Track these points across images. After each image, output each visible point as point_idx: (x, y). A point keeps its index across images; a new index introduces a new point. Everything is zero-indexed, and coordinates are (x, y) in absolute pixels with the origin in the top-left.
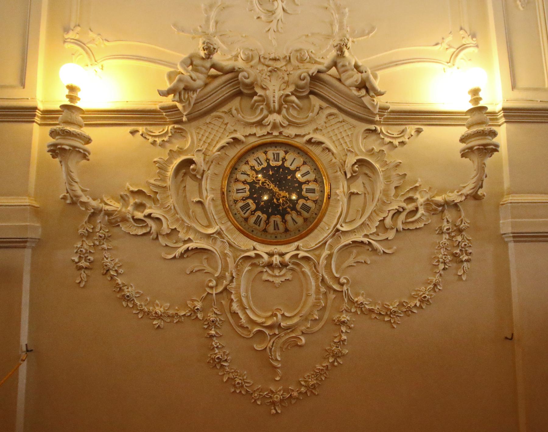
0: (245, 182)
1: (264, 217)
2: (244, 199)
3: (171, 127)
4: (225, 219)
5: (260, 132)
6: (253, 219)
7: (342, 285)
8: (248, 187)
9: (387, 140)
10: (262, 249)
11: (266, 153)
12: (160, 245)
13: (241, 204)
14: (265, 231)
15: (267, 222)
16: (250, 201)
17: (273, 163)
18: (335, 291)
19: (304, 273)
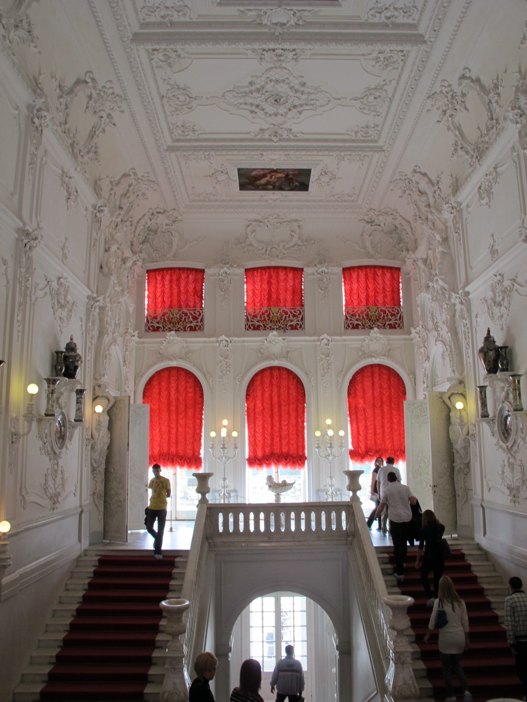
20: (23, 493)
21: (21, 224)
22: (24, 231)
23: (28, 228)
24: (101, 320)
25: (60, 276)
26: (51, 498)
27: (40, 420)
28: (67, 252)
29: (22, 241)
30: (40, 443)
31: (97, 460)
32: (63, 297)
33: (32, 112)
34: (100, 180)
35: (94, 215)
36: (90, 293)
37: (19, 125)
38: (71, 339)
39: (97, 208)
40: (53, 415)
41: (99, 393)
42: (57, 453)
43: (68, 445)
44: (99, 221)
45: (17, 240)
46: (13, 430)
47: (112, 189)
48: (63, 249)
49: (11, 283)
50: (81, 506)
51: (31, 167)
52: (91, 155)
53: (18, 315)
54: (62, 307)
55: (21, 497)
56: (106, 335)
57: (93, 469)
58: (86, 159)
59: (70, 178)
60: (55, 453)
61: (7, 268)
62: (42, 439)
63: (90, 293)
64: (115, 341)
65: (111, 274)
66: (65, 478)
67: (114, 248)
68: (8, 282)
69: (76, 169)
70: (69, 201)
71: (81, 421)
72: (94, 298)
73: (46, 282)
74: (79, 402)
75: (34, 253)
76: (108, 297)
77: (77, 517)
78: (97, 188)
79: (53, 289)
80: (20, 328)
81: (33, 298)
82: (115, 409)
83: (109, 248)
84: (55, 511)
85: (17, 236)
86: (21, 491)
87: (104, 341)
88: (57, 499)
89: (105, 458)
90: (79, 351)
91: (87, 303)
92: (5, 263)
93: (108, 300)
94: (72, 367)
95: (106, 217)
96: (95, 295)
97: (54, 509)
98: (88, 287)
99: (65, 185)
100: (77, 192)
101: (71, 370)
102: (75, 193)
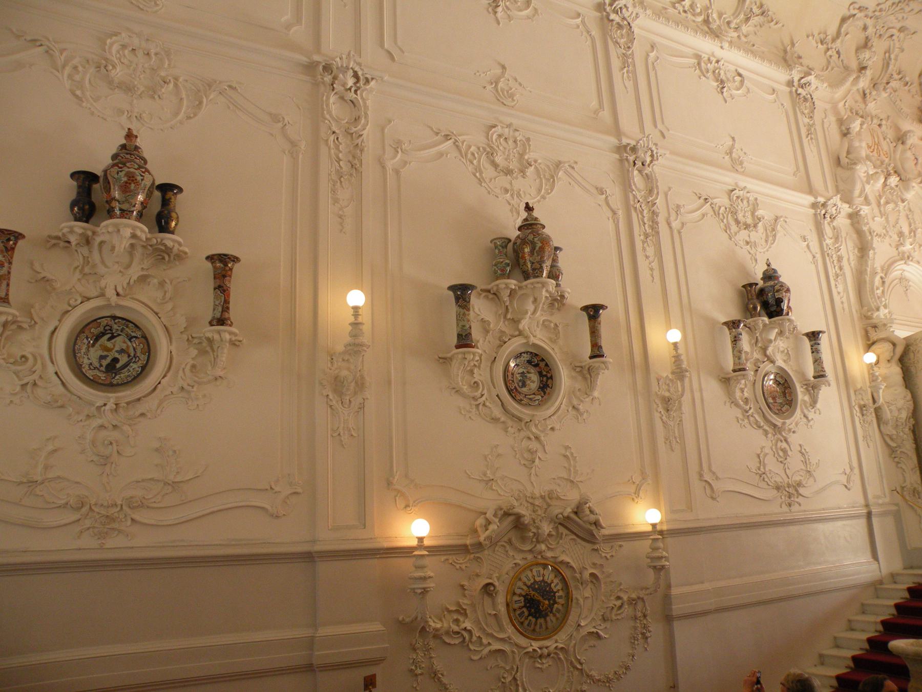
0: (520, 595)
1: (533, 620)
2: (520, 608)
3: (472, 556)
4: (510, 625)
5: (530, 557)
6: (526, 623)
7: (581, 664)
8: (522, 599)
9: (603, 555)
10: (536, 645)
11: (531, 570)
12: (470, 650)
13: (518, 612)
14: (534, 630)
15: (536, 624)
16: (525, 610)
17: (537, 579)
18: (578, 669)
19: (560, 659)
20: (707, 477)
21: (613, 141)
22: (625, 147)
23: (625, 141)
24: (860, 233)
25: (731, 188)
26: (778, 488)
27: (726, 381)
28: (741, 154)
29: (627, 160)
30: (738, 413)
31: (894, 437)
32: (749, 214)
33: (605, 10)
34: (793, 44)
35: (795, 95)
36: (811, 199)
37: (588, 32)
38: (768, 266)
39: (796, 84)
40: (744, 370)
41: (874, 336)
42: (779, 424)
43: (811, 415)
44: (809, 99)
45: (621, 161)
46: (667, 394)
47: (828, 49)
48: (730, 153)
49: (620, 212)
50: (867, 506)
51: (625, 70)
52: (755, 20)
53: (644, 249)
54: (747, 226)
55: (704, 483)
56: (871, 252)
57: (892, 452)
58: (744, 29)
59: (718, 62)
60: (775, 426)
61: (607, 197)
62: (737, 405)
63: (811, 199)
64: (906, 258)
65: (855, 164)
66: (814, 461)
67: (856, 126)
68: (614, 213)
69: (722, 47)
70: (725, 90)
71: (823, 376)
72: (824, 205)
73: (702, 200)
74: (815, 351)
75: (657, 169)
76: (860, 196)
77: (863, 522)
78: (786, 57)
79: (720, 207)
80: (655, 265)
81: (675, 225)
82: (911, 355)
83: (848, 129)
84: (795, 508)
85: (617, 156)
86: (701, 475)
87: (870, 263)
88: (797, 491)
89: (907, 430)
90: (785, 278)
91: (815, 215)
92: (601, 191)
93: (858, 201)
94: (771, 301)
95: (819, 89)
96: (821, 200)
97: (790, 505)
98: (811, 191)
99: (710, 74)
100: (740, 75)
101: (772, 306)
102: (738, 78)
